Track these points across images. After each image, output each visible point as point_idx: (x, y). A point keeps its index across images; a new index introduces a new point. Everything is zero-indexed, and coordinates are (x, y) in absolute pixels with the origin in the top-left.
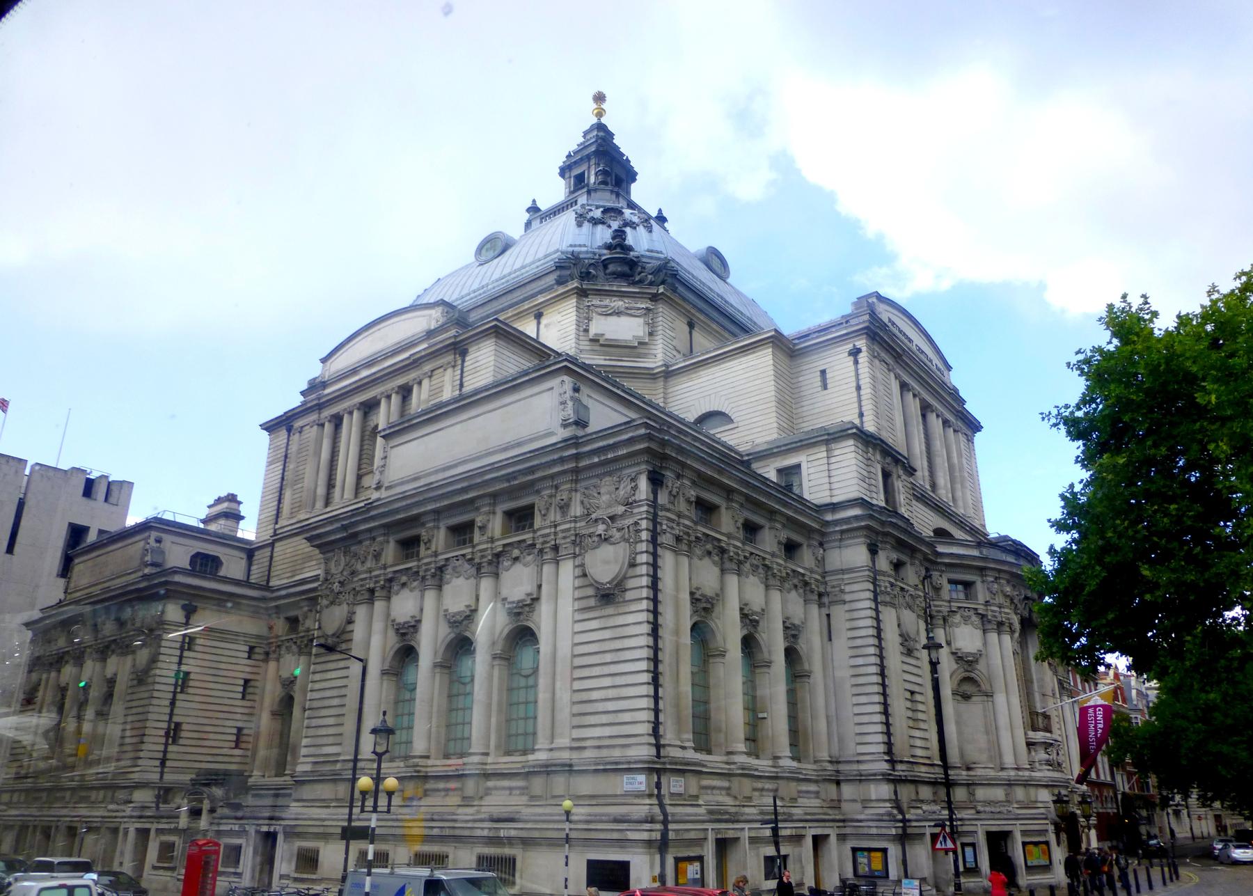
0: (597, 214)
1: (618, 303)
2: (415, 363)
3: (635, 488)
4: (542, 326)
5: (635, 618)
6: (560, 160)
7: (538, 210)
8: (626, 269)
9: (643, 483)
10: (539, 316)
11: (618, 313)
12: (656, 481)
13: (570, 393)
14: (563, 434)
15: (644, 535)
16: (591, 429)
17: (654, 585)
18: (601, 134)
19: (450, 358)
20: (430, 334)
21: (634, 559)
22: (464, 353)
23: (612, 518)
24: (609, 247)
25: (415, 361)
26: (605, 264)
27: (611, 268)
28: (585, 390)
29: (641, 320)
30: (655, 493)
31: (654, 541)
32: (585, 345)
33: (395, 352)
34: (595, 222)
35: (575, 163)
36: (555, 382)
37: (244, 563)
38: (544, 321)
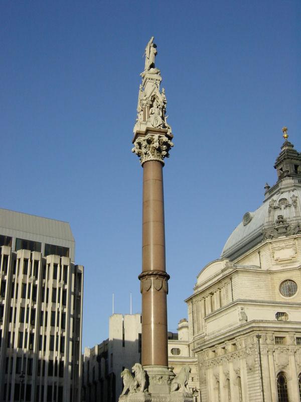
0: (276, 204)
1: (283, 245)
2: (219, 281)
3: (253, 340)
4: (261, 256)
5: (257, 375)
6: (274, 162)
7: (269, 187)
8: (284, 230)
9: (256, 339)
10: (259, 253)
11: (283, 248)
12: (259, 337)
13: (240, 311)
14: (239, 323)
15: (257, 353)
16: (248, 321)
17: (261, 366)
18: (287, 148)
19: (227, 280)
20: (223, 271)
21: (255, 359)
22: (231, 279)
23: (250, 348)
24: (278, 222)
25: (220, 281)
26: (277, 230)
27: (280, 231)
28: (245, 308)
29: (292, 249)
30: (259, 341)
31: (260, 353)
32: (274, 262)
33: (215, 277)
34: (275, 208)
35: (279, 164)
36: (236, 308)
37: (188, 348)
38: (261, 254)
